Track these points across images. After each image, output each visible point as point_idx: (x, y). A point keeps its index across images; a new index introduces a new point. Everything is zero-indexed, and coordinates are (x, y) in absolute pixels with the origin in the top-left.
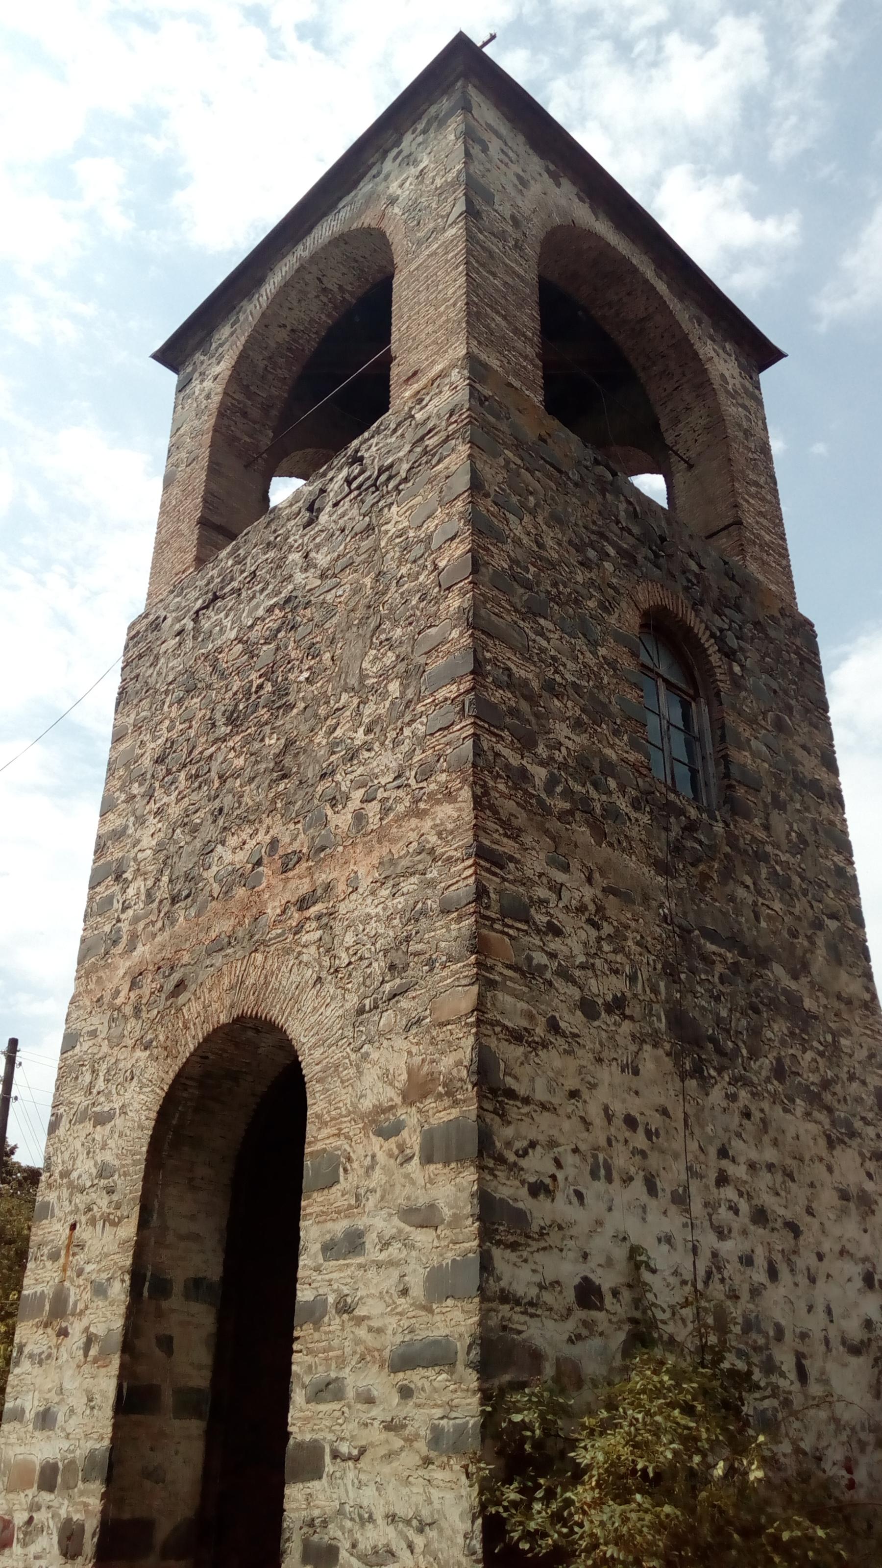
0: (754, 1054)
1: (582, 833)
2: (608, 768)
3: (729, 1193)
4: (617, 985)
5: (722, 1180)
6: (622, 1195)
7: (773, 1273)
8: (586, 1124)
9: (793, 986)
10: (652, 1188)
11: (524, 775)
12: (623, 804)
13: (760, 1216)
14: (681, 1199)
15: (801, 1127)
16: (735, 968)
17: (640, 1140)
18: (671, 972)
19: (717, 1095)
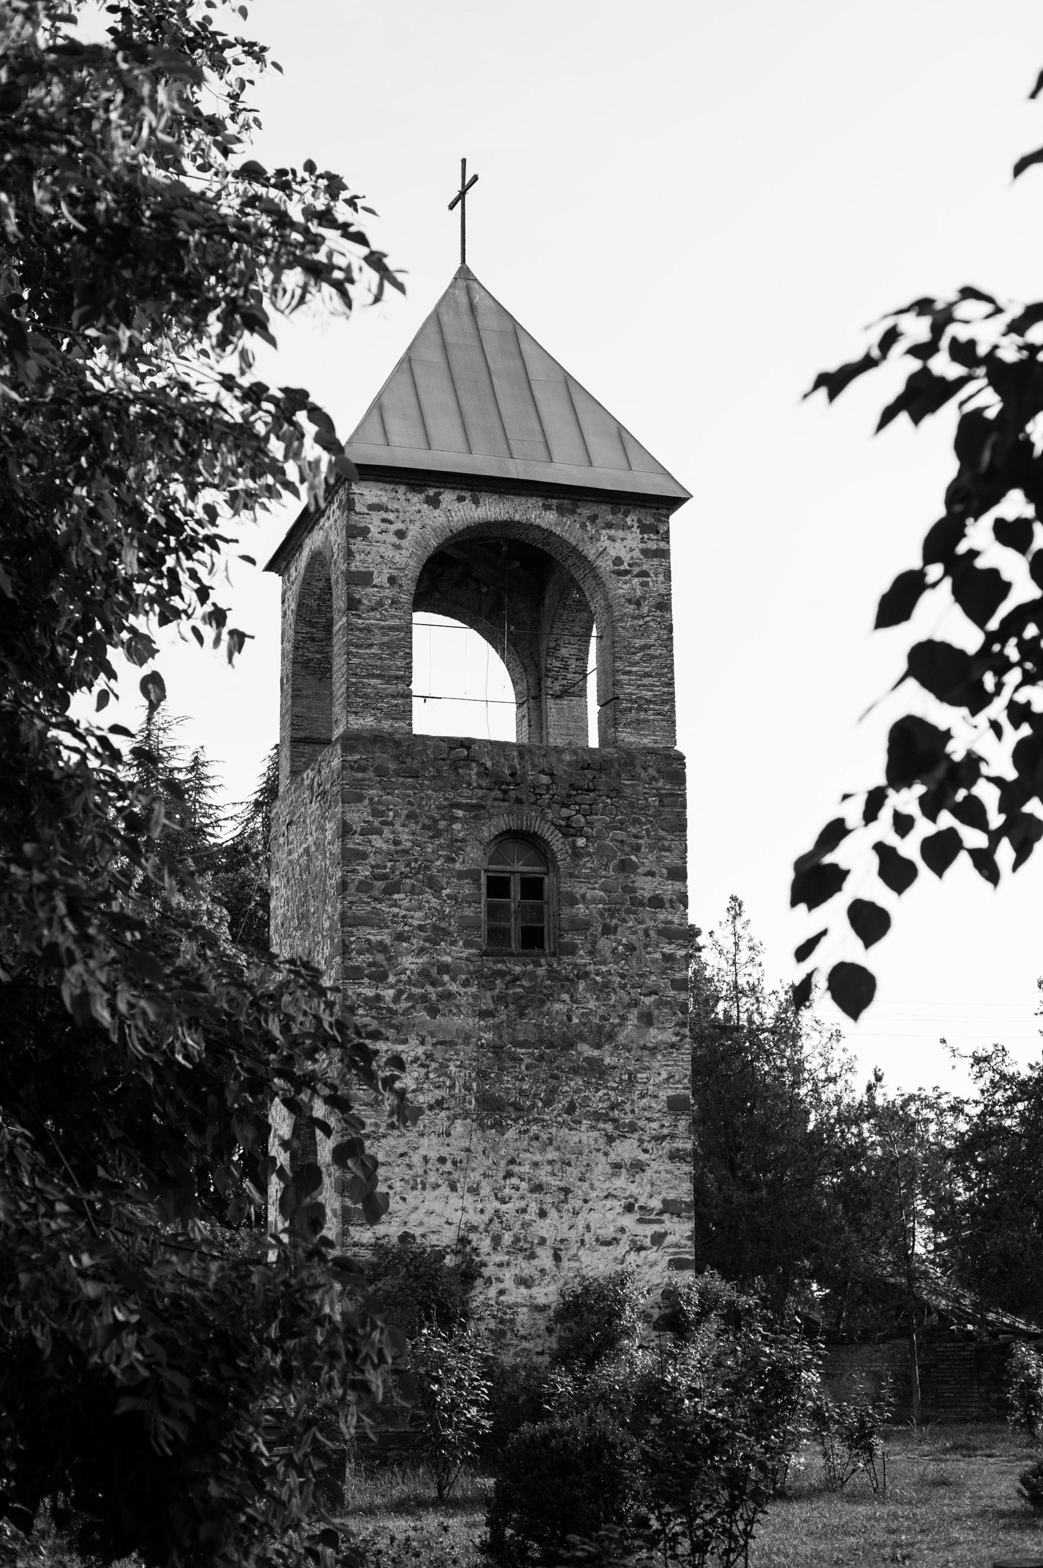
0: (548, 1103)
1: (422, 1015)
2: (444, 968)
3: (514, 1181)
4: (439, 1094)
5: (509, 1175)
6: (430, 1194)
7: (543, 1214)
8: (410, 1166)
9: (596, 1053)
10: (453, 1188)
11: (378, 998)
12: (454, 988)
13: (538, 1188)
14: (474, 1190)
15: (585, 1135)
16: (541, 1058)
17: (448, 1166)
18: (483, 1075)
19: (511, 1134)
